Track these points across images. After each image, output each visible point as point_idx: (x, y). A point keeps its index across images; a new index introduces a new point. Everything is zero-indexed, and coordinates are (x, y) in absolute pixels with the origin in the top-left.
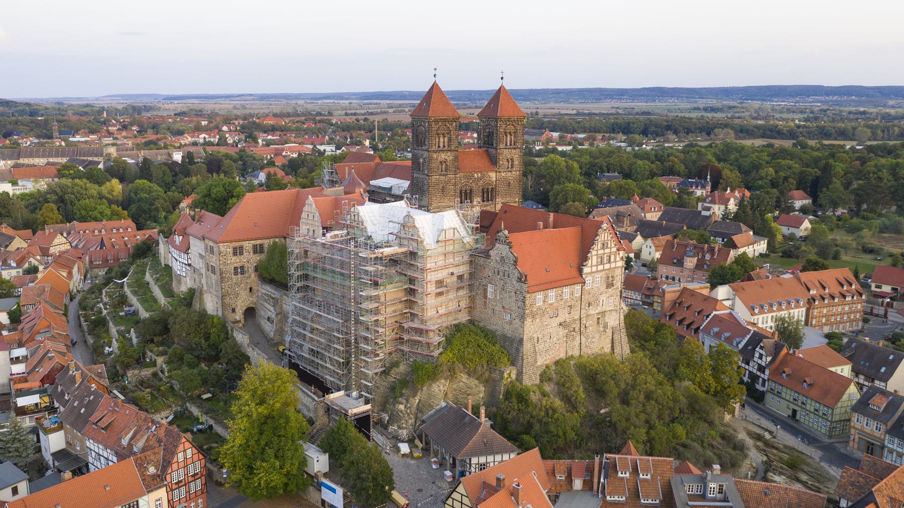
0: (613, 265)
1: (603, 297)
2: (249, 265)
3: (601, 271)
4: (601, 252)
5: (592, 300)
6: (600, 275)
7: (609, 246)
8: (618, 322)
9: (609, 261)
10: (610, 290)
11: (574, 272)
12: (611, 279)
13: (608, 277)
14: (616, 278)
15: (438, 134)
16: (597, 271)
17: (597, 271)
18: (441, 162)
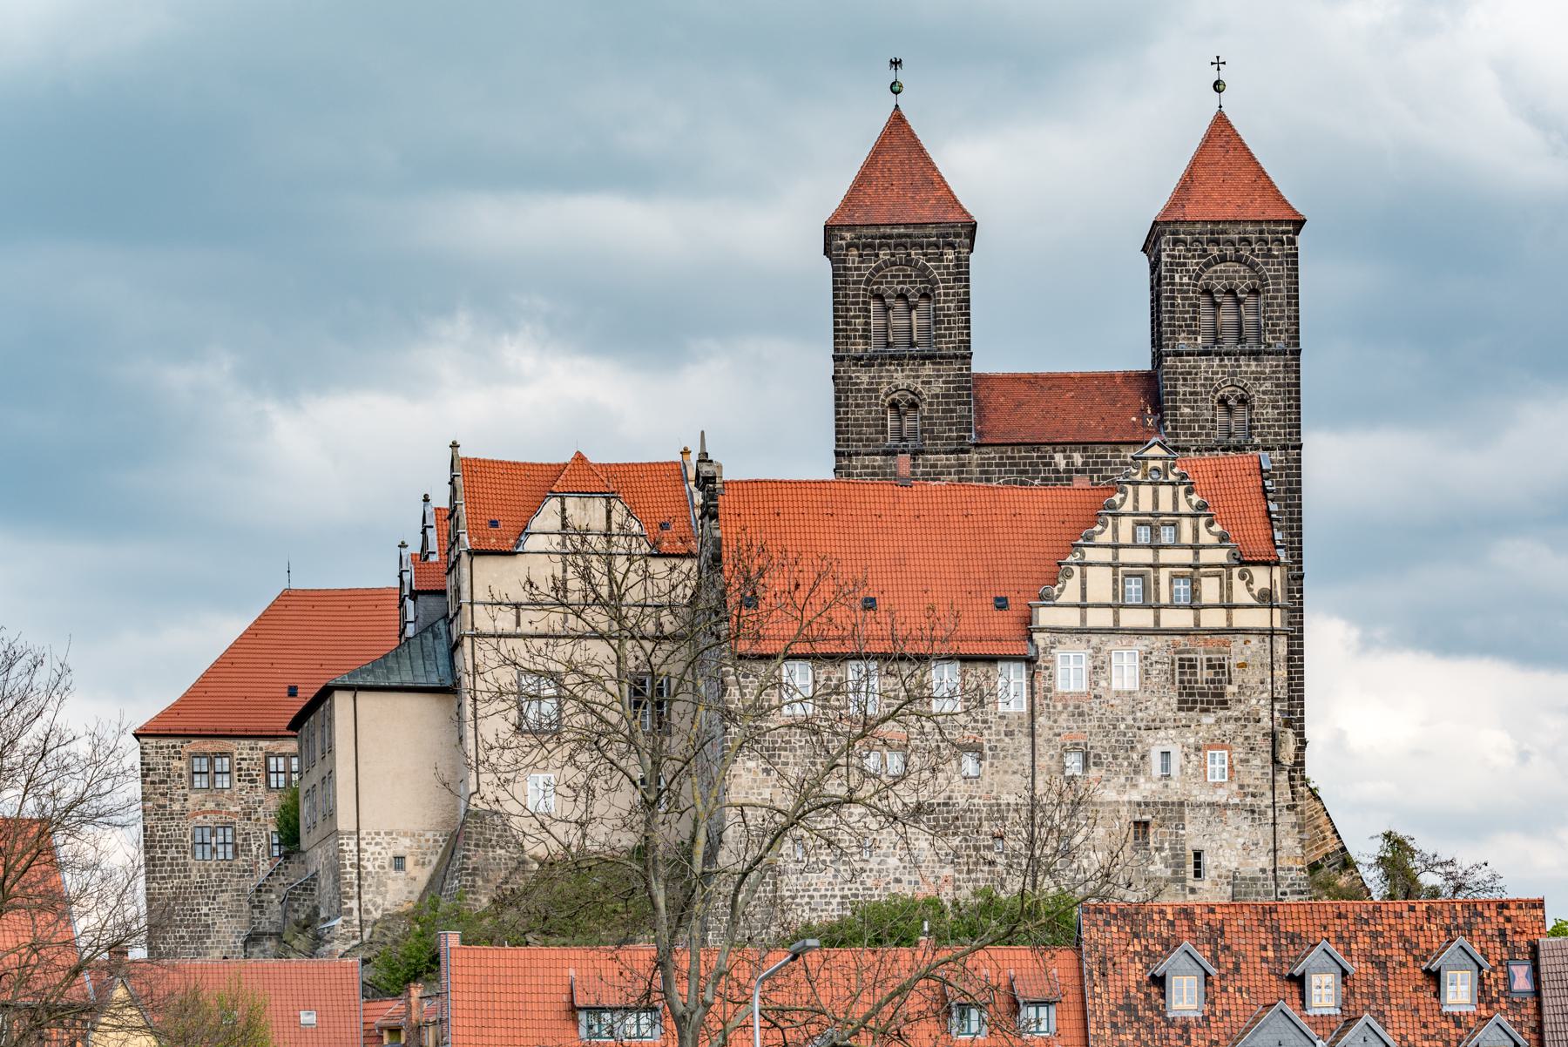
0: (1214, 619)
1: (1155, 744)
2: (250, 827)
3: (1139, 632)
4: (1146, 556)
5: (1098, 743)
6: (1141, 644)
7: (1187, 537)
8: (1264, 861)
9: (1195, 605)
10: (1208, 719)
11: (1004, 623)
12: (1204, 674)
13: (1187, 665)
14: (1237, 675)
15: (879, 297)
16: (1115, 631)
17: (1115, 631)
18: (894, 405)
